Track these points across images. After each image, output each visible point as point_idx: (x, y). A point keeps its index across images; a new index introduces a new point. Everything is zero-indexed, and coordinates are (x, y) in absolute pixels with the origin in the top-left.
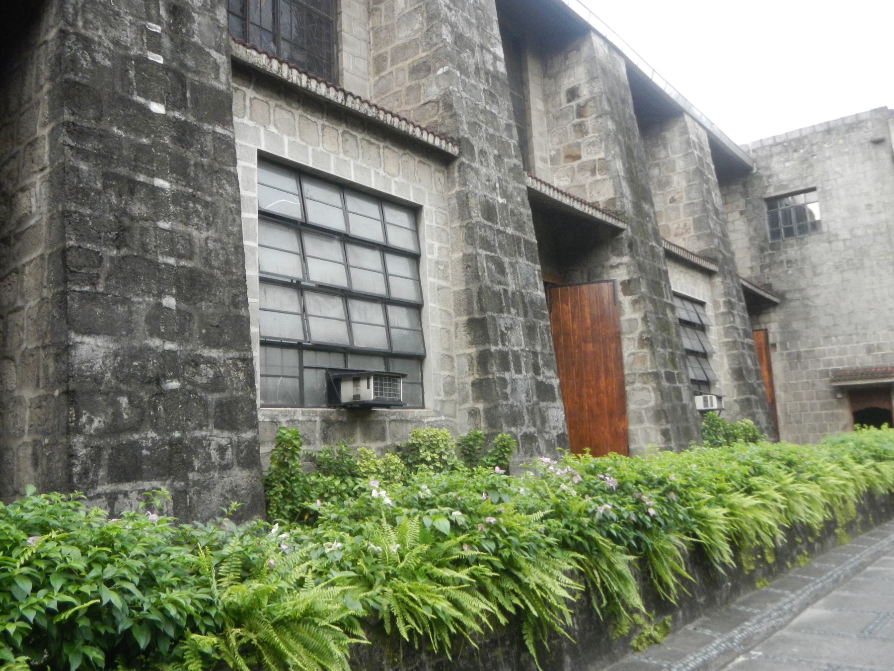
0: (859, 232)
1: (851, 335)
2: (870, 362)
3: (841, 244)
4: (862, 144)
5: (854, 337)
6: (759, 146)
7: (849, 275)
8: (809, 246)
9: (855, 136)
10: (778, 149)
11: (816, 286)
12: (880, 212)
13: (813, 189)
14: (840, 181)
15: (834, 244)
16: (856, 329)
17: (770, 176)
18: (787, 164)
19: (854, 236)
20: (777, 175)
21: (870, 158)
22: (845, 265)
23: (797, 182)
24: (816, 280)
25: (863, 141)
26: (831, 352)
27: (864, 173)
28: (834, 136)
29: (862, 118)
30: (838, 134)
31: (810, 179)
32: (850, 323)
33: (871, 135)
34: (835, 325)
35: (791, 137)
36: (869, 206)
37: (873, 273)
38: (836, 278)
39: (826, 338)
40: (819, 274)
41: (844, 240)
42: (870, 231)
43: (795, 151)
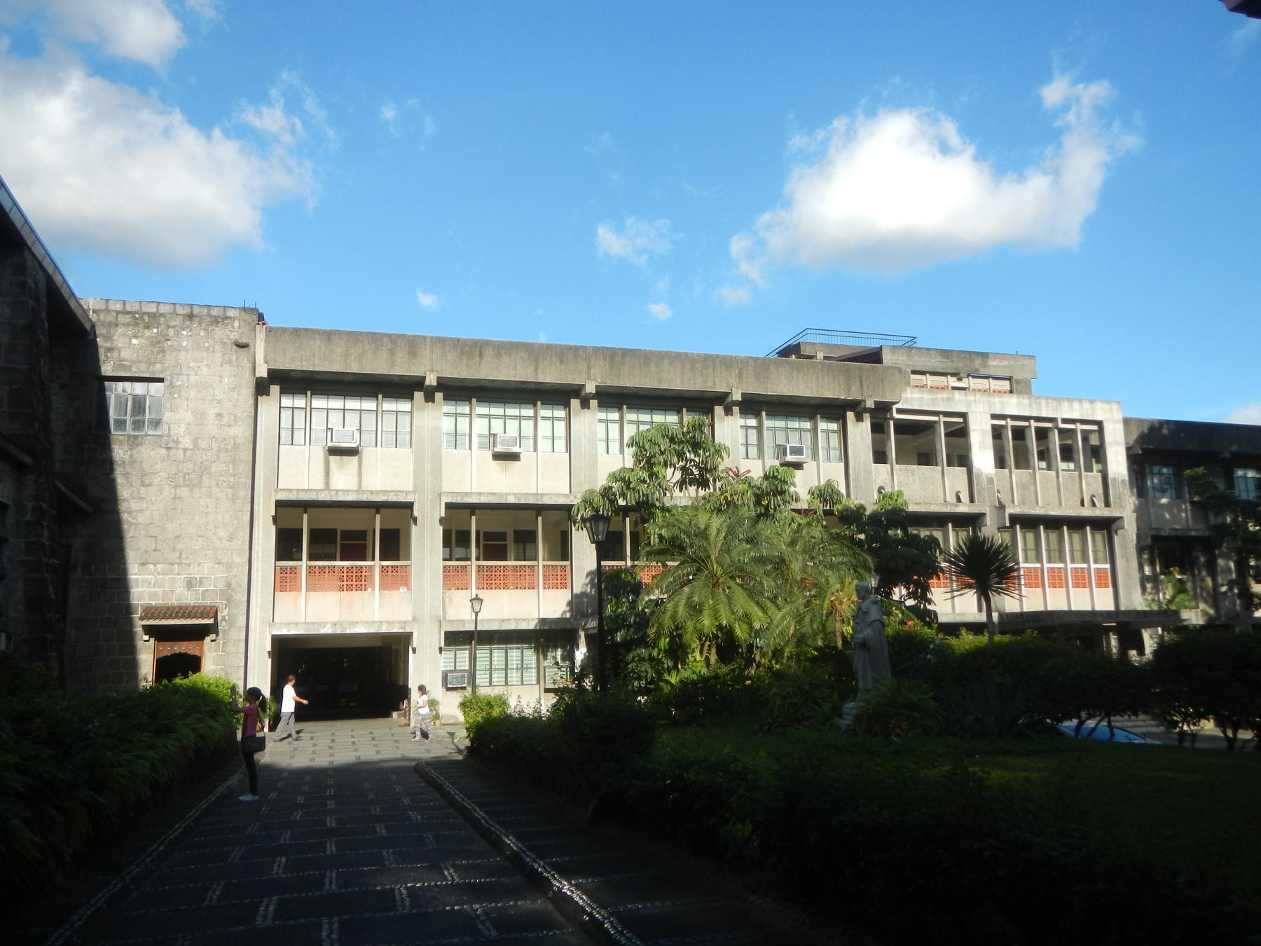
0: (203, 444)
2: (189, 598)
3: (181, 451)
4: (225, 343)
5: (176, 566)
6: (104, 307)
7: (183, 492)
8: (142, 449)
9: (219, 332)
10: (127, 319)
11: (141, 499)
12: (230, 426)
13: (161, 380)
14: (193, 378)
15: (172, 452)
16: (180, 558)
17: (110, 350)
18: (134, 341)
19: (196, 447)
20: (120, 350)
21: (230, 362)
22: (181, 479)
23: (143, 366)
25: (225, 340)
26: (146, 580)
27: (221, 377)
28: (196, 325)
29: (231, 313)
30: (200, 323)
31: (158, 366)
32: (174, 550)
33: (235, 336)
35: (145, 310)
36: (219, 415)
37: (210, 495)
38: (168, 492)
39: (143, 564)
40: (148, 485)
41: (185, 450)
42: (215, 446)
43: (148, 327)
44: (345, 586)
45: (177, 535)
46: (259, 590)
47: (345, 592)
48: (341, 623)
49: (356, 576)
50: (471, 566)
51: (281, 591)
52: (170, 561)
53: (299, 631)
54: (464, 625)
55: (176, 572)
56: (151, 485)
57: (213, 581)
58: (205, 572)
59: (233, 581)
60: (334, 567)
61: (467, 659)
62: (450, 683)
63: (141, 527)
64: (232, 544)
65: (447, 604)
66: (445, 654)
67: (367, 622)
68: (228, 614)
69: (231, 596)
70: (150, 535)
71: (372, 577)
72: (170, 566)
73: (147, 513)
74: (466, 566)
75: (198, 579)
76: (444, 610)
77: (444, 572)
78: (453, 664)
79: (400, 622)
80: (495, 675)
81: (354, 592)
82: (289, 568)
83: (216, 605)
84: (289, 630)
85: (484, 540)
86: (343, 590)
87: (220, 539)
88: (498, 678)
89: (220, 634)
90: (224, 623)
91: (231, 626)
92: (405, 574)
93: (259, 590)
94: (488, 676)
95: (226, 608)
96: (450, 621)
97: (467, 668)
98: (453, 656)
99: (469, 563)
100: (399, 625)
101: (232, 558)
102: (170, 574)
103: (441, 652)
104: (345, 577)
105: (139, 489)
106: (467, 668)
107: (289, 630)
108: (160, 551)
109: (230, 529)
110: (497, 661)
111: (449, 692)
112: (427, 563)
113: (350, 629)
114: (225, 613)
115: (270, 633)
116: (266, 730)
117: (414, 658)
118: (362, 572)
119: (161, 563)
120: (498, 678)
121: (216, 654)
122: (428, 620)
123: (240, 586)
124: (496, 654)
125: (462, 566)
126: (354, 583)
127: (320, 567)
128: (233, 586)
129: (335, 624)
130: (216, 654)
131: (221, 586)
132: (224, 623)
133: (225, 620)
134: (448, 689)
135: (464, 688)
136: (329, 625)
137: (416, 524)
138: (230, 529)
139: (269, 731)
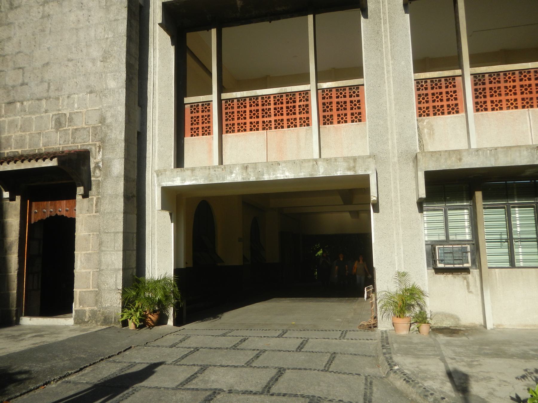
1: (39, 100)
5: (44, 102)
11: (9, 24)
16: (48, 91)
24: (11, 16)
32: (42, 81)
34: (22, 84)
39: (10, 103)
40: (16, 8)
44: (273, 123)
45: (46, 62)
46: (157, 132)
47: (273, 130)
48: (255, 165)
49: (287, 108)
50: (462, 76)
51: (192, 136)
52: (38, 96)
53: (196, 180)
54: (460, 160)
55: (43, 110)
56: (19, 6)
57: (84, 117)
58: (76, 106)
59: (109, 115)
60: (257, 97)
61: (467, 224)
62: (441, 261)
63: (8, 57)
64: (106, 64)
65: (426, 137)
66: (427, 210)
67: (294, 162)
68: (102, 160)
69: (106, 135)
70: (18, 66)
71: (306, 109)
72: (37, 102)
73: (15, 40)
74: (454, 77)
75: (68, 115)
76: (421, 145)
77: (418, 89)
78: (443, 231)
79: (346, 159)
80: (519, 250)
81: (286, 129)
82: (200, 104)
83: (88, 148)
84: (183, 180)
85: (471, 66)
86: (270, 128)
87: (93, 61)
88: (524, 254)
89: (94, 188)
90: (97, 171)
91: (107, 174)
92: (357, 99)
93: (157, 132)
94: (506, 250)
95: (99, 151)
96: (433, 153)
97: (468, 237)
98: (442, 218)
99: (458, 72)
100: (345, 165)
101: (106, 84)
102: (37, 112)
103: (421, 210)
104: (272, 111)
105: (7, 15)
106: (468, 237)
107: (183, 180)
108: (27, 84)
109: (104, 46)
110: (521, 226)
111: (441, 277)
112: (388, 72)
113: (269, 174)
114: (99, 157)
115: (159, 185)
116: (170, 322)
117: (375, 219)
118: (294, 102)
119: (29, 100)
120: (524, 254)
121: (88, 214)
122: (396, 159)
123: (116, 121)
124: (517, 215)
125: (446, 78)
126: (285, 117)
127: (238, 99)
128: (109, 120)
129: (246, 168)
130: (88, 214)
131: (94, 121)
132: (97, 171)
133: (99, 167)
134: (438, 271)
135: (466, 270)
136: (237, 169)
137: (366, 17)
138: (104, 46)
139: (174, 325)
